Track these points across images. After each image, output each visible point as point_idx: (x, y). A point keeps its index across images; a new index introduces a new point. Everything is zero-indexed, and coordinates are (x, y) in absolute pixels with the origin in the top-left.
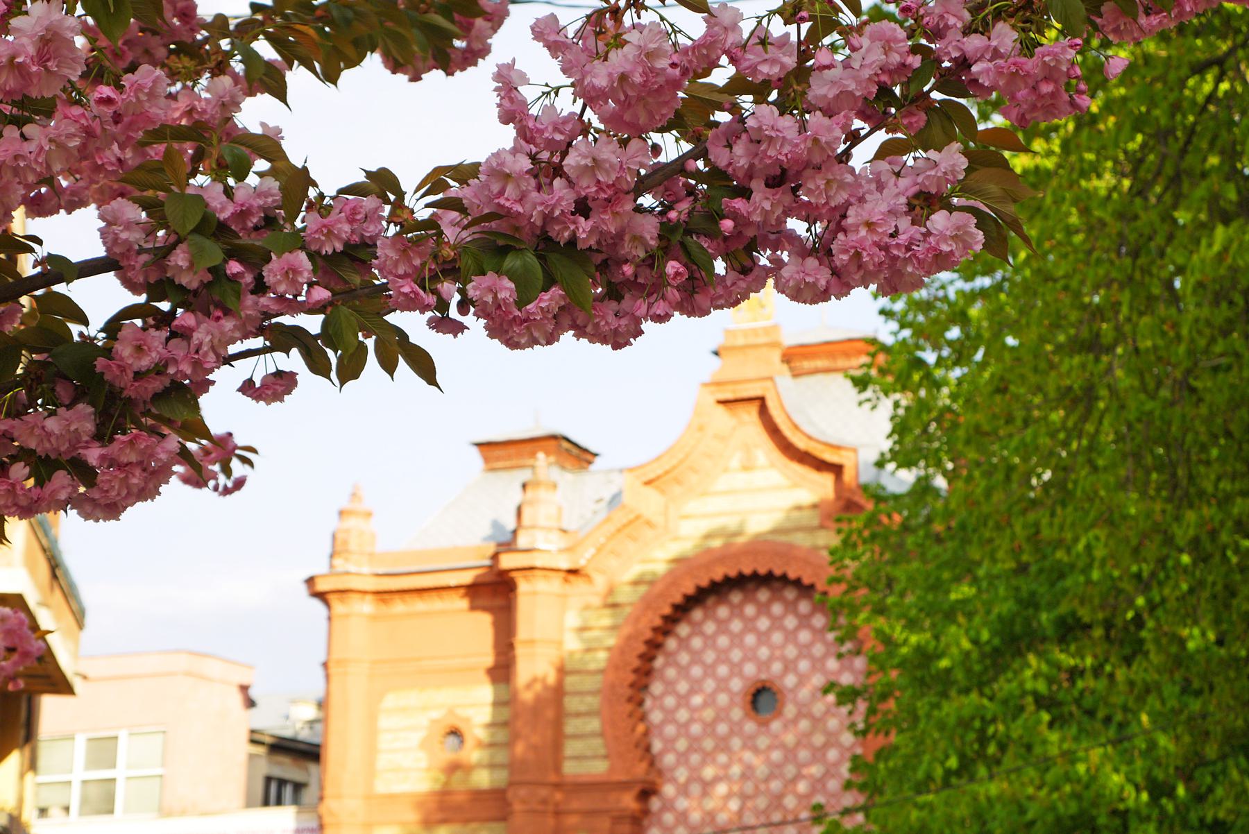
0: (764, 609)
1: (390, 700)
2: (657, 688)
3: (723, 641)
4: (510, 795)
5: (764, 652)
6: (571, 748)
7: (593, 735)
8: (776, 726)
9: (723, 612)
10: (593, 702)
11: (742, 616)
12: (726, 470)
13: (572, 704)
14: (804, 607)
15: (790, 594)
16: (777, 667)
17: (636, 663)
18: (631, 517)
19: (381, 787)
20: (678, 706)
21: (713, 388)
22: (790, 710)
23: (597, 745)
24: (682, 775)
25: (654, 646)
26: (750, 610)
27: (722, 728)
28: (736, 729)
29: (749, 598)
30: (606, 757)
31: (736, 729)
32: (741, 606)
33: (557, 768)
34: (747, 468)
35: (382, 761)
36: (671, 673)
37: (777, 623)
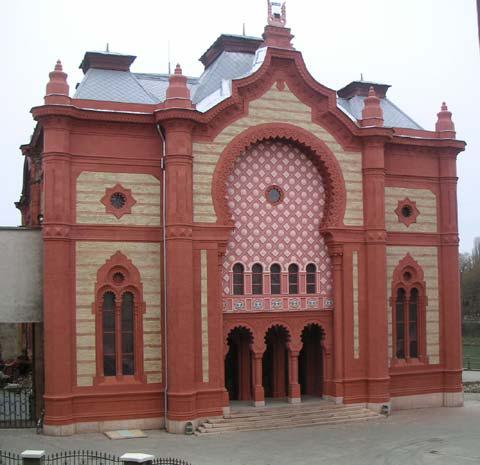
0: (274, 154)
1: (81, 177)
6: (197, 209)
7: (208, 204)
14: (291, 155)
15: (285, 149)
16: (280, 180)
20: (235, 194)
22: (286, 200)
23: (211, 209)
26: (268, 154)
28: (262, 206)
29: (267, 148)
31: (262, 206)
34: (280, 88)
35: (79, 208)
37: (280, 161)
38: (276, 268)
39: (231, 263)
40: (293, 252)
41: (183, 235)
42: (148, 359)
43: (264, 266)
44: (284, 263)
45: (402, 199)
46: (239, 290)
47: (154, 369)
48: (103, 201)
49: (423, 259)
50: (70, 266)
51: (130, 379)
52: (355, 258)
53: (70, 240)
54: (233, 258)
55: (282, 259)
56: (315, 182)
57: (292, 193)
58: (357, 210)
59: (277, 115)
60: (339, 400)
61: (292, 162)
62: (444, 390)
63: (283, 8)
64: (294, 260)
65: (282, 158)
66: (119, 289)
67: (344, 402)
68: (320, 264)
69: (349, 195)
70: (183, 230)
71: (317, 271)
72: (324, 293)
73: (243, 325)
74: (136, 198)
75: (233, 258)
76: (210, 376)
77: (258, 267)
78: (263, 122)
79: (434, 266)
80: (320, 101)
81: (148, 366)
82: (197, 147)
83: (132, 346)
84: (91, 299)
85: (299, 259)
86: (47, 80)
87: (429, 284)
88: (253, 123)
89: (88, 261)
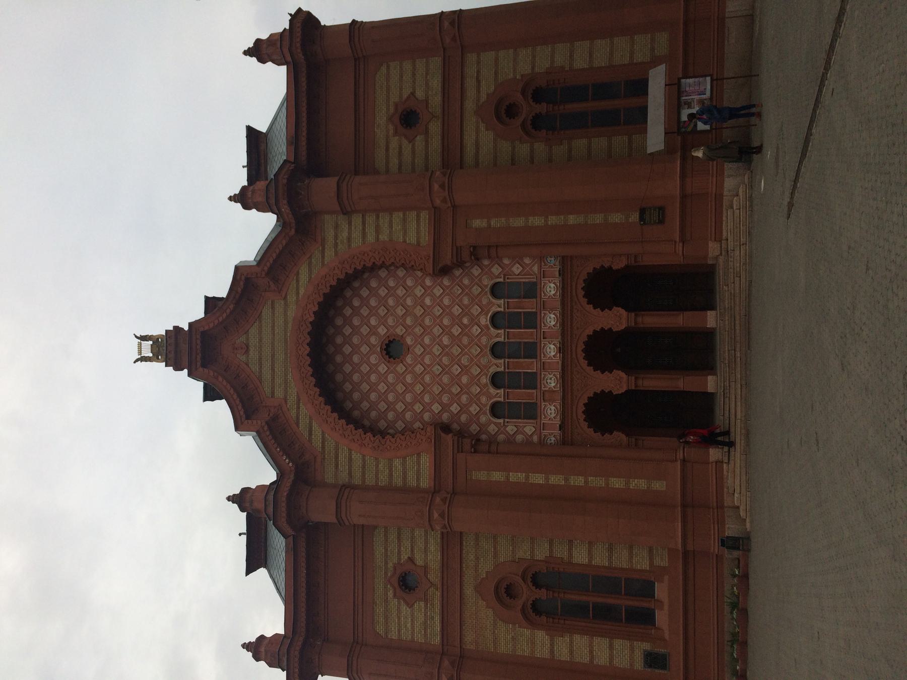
1: (380, 629)
2: (382, 424)
3: (356, 377)
6: (412, 482)
7: (404, 464)
8: (409, 341)
9: (339, 377)
12: (247, 364)
13: (383, 480)
14: (339, 321)
18: (266, 428)
19: (437, 640)
20: (395, 410)
22: (400, 331)
24: (436, 408)
25: (357, 424)
26: (339, 359)
30: (419, 455)
35: (419, 638)
36: (373, 414)
38: (496, 351)
39: (490, 422)
40: (474, 321)
41: (442, 515)
43: (493, 370)
45: (391, 127)
46: (530, 412)
48: (411, 606)
49: (483, 83)
51: (661, 591)
52: (477, 223)
54: (483, 419)
55: (484, 340)
57: (390, 321)
58: (404, 220)
60: (713, 249)
64: (485, 320)
66: (527, 593)
69: (384, 237)
70: (436, 515)
71: (501, 280)
72: (536, 269)
73: (581, 408)
74: (405, 557)
79: (497, 59)
81: (641, 562)
84: (541, 636)
85: (483, 311)
86: (262, 663)
87: (524, 68)
88: (293, 392)
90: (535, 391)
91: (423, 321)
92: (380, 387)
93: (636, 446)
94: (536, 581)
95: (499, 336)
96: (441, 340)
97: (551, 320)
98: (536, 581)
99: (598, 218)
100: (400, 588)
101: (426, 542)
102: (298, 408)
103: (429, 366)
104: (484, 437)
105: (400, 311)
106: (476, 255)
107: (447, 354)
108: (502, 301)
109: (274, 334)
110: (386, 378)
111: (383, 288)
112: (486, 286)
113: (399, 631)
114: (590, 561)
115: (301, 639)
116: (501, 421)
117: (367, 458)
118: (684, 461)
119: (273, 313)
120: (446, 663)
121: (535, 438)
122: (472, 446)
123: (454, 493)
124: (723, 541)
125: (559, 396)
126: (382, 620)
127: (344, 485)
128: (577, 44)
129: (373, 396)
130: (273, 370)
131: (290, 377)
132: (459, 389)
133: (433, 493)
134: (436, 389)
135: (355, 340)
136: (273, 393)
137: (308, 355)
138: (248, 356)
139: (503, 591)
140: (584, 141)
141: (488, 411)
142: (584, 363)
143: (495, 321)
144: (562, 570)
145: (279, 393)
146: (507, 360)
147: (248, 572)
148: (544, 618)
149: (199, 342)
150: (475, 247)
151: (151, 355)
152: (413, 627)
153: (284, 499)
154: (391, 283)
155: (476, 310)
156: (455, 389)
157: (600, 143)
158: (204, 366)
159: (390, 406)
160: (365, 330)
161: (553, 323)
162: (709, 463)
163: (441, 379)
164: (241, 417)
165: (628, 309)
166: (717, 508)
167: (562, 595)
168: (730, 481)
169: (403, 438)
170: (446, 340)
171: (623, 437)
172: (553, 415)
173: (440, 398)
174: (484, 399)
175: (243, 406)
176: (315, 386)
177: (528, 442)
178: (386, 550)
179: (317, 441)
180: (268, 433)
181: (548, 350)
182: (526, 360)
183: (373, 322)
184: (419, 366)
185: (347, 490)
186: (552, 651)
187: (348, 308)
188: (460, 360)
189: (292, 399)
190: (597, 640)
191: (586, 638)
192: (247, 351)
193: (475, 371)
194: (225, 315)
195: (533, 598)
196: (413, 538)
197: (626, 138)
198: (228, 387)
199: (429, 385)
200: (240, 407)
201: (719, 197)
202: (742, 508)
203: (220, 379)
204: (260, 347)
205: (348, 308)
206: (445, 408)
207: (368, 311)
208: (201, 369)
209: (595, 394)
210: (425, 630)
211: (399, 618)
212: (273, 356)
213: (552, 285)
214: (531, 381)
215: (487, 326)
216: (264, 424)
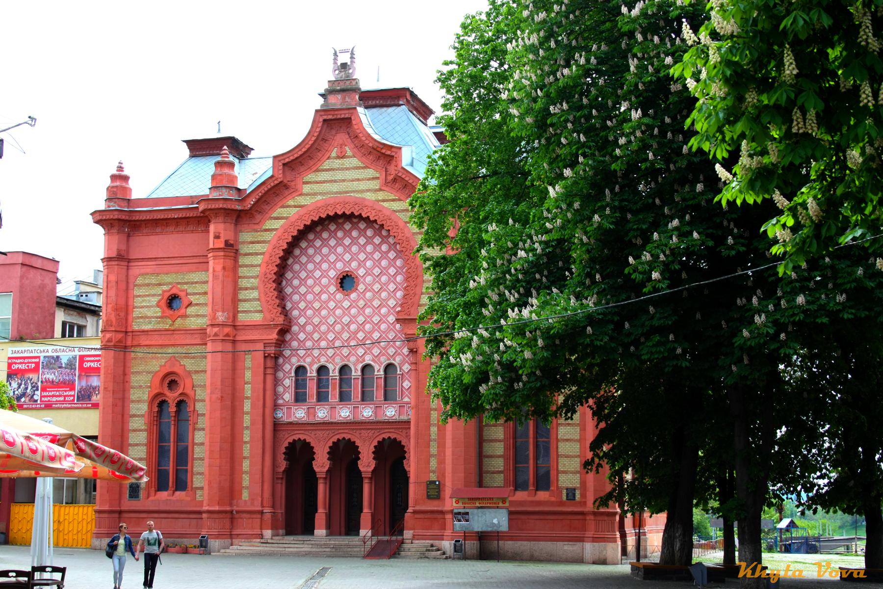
0: (347, 233)
1: (140, 280)
2: (289, 275)
3: (325, 250)
4: (208, 330)
5: (347, 257)
6: (242, 306)
8: (353, 296)
9: (325, 235)
10: (255, 282)
11: (336, 237)
12: (329, 158)
13: (243, 283)
14: (369, 233)
15: (362, 225)
16: (354, 264)
17: (278, 262)
18: (276, 182)
19: (136, 328)
21: (323, 113)
22: (361, 287)
23: (256, 305)
24: (302, 321)
26: (340, 234)
27: (324, 297)
29: (340, 227)
30: (261, 311)
32: (335, 232)
33: (235, 317)
34: (342, 156)
35: (136, 313)
37: (354, 241)
41: (216, 335)
42: (199, 474)
43: (330, 367)
44: (355, 365)
46: (300, 398)
47: (201, 485)
48: (158, 305)
50: (125, 374)
53: (126, 347)
56: (399, 263)
57: (369, 279)
59: (335, 187)
61: (369, 240)
62: (581, 540)
63: (352, 58)
64: (368, 360)
65: (359, 237)
66: (172, 397)
67: (414, 537)
68: (402, 364)
70: (216, 330)
71: (398, 372)
72: (406, 399)
74: (192, 298)
75: (294, 360)
76: (250, 495)
77: (322, 370)
78: (319, 198)
80: (389, 163)
81: (198, 481)
82: (246, 236)
83: (183, 457)
84: (143, 408)
86: (108, 182)
89: (141, 368)
90: (315, 400)
91: (369, 307)
92: (318, 272)
93: (277, 478)
94: (180, 404)
95: (356, 372)
96: (354, 323)
97: (367, 413)
98: (180, 404)
99: (434, 450)
100: (171, 295)
101: (203, 316)
102: (295, 206)
103: (334, 313)
104: (281, 360)
105: (377, 287)
106: (411, 351)
107: (343, 328)
108: (382, 373)
109: (353, 181)
110: (325, 277)
111: (395, 271)
112: (394, 360)
113: (139, 296)
114: (197, 444)
115: (127, 218)
116: (293, 374)
117: (258, 269)
118: (262, 513)
119: (369, 179)
120: (120, 336)
121: (280, 402)
122: (269, 354)
123: (234, 342)
124: (204, 537)
125: (311, 420)
126: (147, 281)
127: (237, 250)
128: (578, 429)
129: (310, 266)
130: (324, 182)
131: (319, 198)
132: (316, 339)
133: (234, 326)
134: (316, 320)
135: (354, 249)
136: (307, 183)
137: (336, 213)
138: (335, 159)
139: (173, 378)
140: (501, 436)
141: (299, 364)
142: (335, 439)
143: (366, 368)
144: (190, 422)
145: (306, 189)
146: (338, 378)
147: (186, 142)
148: (156, 409)
149: (343, 116)
150: (416, 351)
151: (339, 64)
152: (142, 307)
153: (221, 206)
154: (399, 278)
155: (376, 351)
156: (316, 336)
157: (499, 449)
158: (325, 121)
159: (303, 282)
160: (362, 256)
161: (365, 414)
162: (261, 529)
163: (324, 323)
164: (284, 159)
165: (373, 472)
166: (231, 535)
167: (173, 422)
168: (247, 544)
169: (274, 298)
170: (353, 327)
171: (282, 469)
172: (297, 416)
173: (310, 324)
174: (309, 360)
175: (293, 160)
176: (312, 220)
177: (276, 395)
178: (196, 283)
179: (269, 224)
180: (272, 184)
181: (344, 411)
182: (338, 393)
183: (369, 264)
184: (334, 305)
185: (232, 254)
186: (134, 416)
187: (380, 240)
188: (338, 339)
189: (302, 201)
190: (144, 449)
191: (145, 441)
192: (338, 157)
193: (330, 352)
194: (364, 139)
195: (170, 401)
196: (206, 304)
197: (502, 469)
198: (308, 146)
199: (320, 313)
200: (292, 158)
201: (441, 538)
202: (227, 551)
203: (314, 139)
204: (342, 169)
205: (380, 240)
206: (303, 328)
207: (377, 259)
208: (321, 120)
209: (313, 448)
210: (142, 317)
211: (148, 296)
212: (335, 181)
213: (393, 413)
214: (322, 397)
215: (364, 361)
216: (280, 180)
